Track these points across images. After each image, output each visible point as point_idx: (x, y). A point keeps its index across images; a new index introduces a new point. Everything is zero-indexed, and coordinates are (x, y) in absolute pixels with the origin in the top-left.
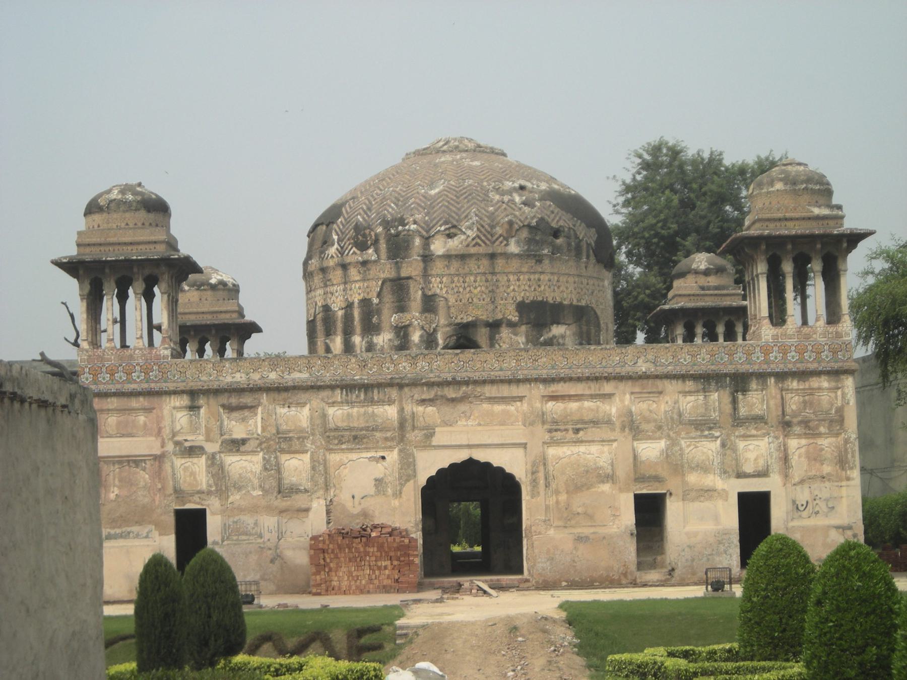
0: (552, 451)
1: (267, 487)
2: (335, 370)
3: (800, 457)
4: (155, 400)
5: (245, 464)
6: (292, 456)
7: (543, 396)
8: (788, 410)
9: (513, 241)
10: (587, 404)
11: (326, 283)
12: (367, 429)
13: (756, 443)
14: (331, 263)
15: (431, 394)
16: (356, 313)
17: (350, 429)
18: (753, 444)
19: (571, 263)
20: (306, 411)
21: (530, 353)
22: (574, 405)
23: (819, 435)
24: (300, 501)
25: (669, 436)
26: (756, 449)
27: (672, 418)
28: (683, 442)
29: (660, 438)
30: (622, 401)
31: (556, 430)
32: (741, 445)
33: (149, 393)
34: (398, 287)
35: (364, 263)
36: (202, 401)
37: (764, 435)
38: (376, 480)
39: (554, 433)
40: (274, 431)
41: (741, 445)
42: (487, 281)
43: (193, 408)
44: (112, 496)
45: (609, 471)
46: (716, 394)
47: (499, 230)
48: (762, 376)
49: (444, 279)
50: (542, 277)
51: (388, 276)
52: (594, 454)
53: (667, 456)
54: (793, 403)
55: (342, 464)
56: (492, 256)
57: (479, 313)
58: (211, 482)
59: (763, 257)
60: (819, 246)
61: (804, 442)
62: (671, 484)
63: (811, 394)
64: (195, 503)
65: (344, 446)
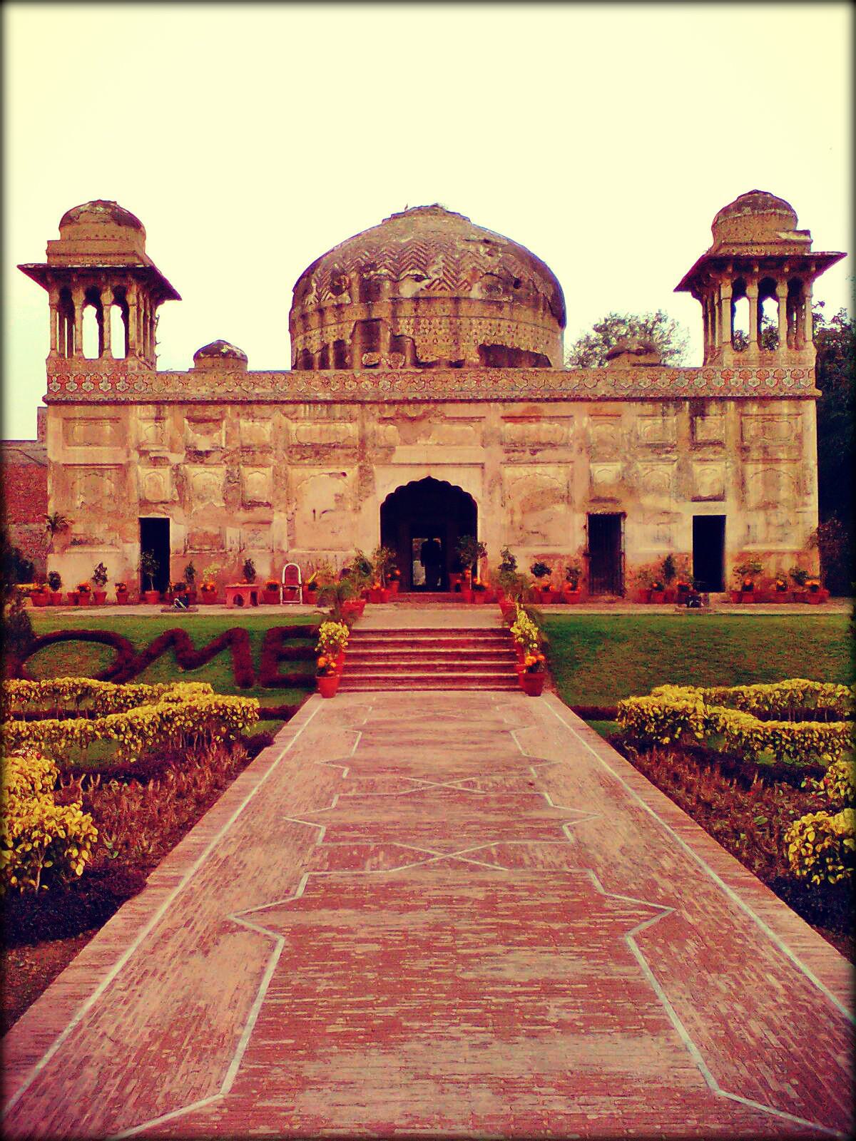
0: (509, 472)
1: (230, 499)
2: (299, 386)
3: (757, 482)
4: (121, 409)
5: (209, 476)
6: (256, 469)
7: (502, 417)
8: (747, 436)
9: (476, 286)
10: (545, 425)
11: (306, 328)
12: (329, 446)
13: (713, 467)
14: (310, 309)
15: (390, 412)
16: (331, 355)
17: (313, 445)
18: (710, 467)
19: (529, 312)
20: (268, 427)
21: (491, 374)
22: (533, 427)
23: (778, 460)
24: (260, 513)
25: (625, 458)
26: (712, 473)
27: (629, 441)
28: (639, 466)
29: (616, 461)
30: (580, 423)
31: (514, 451)
32: (697, 468)
33: (116, 403)
34: (369, 329)
35: (339, 307)
36: (167, 410)
37: (722, 459)
38: (336, 495)
39: (511, 454)
40: (238, 445)
41: (697, 468)
42: (451, 323)
43: (158, 419)
44: (78, 503)
45: (564, 492)
46: (675, 419)
47: (463, 276)
48: (722, 400)
49: (412, 321)
50: (502, 323)
51: (359, 318)
52: (550, 475)
53: (623, 478)
54: (752, 428)
55: (303, 479)
56: (457, 300)
57: (443, 353)
58: (175, 491)
59: (728, 281)
60: (787, 270)
61: (761, 467)
62: (627, 505)
63: (772, 420)
64: (158, 512)
65: (306, 462)
